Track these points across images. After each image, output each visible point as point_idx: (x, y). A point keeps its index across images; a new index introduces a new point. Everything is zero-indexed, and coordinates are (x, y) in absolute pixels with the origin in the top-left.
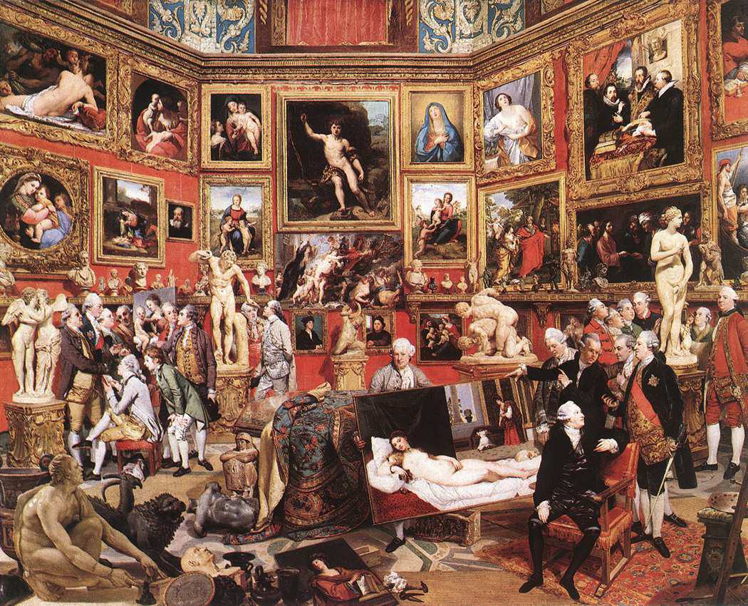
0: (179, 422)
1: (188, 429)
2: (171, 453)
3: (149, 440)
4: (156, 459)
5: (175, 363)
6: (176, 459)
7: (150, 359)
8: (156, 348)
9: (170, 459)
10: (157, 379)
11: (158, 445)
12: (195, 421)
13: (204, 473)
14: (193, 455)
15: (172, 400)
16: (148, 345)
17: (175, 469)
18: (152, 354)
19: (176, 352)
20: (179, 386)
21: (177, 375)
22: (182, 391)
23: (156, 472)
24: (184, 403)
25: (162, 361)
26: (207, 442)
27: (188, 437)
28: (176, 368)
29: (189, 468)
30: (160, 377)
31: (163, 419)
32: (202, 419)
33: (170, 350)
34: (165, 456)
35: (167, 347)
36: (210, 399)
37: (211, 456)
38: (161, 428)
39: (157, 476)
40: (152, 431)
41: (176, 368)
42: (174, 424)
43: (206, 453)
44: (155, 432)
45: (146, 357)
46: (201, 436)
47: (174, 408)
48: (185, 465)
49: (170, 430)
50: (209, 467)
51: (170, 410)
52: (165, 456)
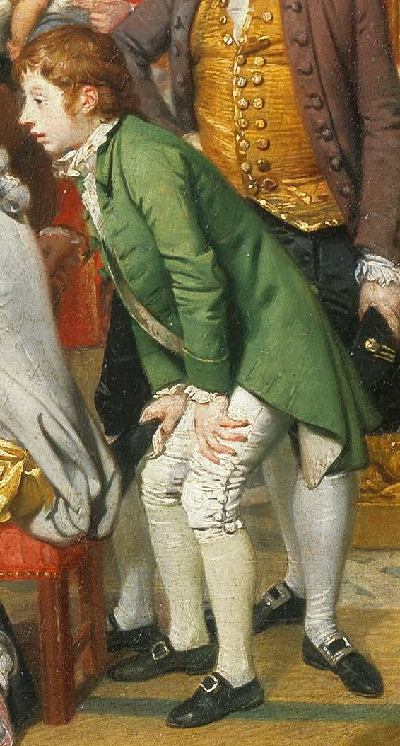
0: (203, 441)
1: (253, 472)
2: (156, 599)
3: (41, 526)
4: (79, 628)
5: (186, 114)
6: (183, 634)
7: (56, 96)
8: (87, 32)
9: (154, 631)
10: (91, 199)
11: (87, 562)
12: (286, 430)
13: (336, 712)
14: (277, 614)
15: (167, 310)
16: (42, 15)
17: (177, 688)
18: (62, 65)
19: (193, 59)
20: (208, 240)
21: (203, 188)
22: (222, 262)
23: (72, 701)
24: (234, 333)
25: (120, 101)
26: (353, 543)
27: (261, 515)
28: (195, 141)
29: (253, 687)
30: (106, 188)
31: (117, 415)
32: (331, 420)
33: (164, 43)
34: (126, 615)
35: (147, 34)
36: (373, 313)
37: (372, 618)
38: (110, 467)
39: (85, 721)
40: (59, 480)
41: (195, 141)
42: (176, 444)
43: (346, 601)
44: (77, 488)
45: (32, 80)
46: (320, 507)
47: (177, 361)
48: (233, 665)
49: (155, 473)
50: (360, 674)
51: (154, 368)
52: (126, 615)
